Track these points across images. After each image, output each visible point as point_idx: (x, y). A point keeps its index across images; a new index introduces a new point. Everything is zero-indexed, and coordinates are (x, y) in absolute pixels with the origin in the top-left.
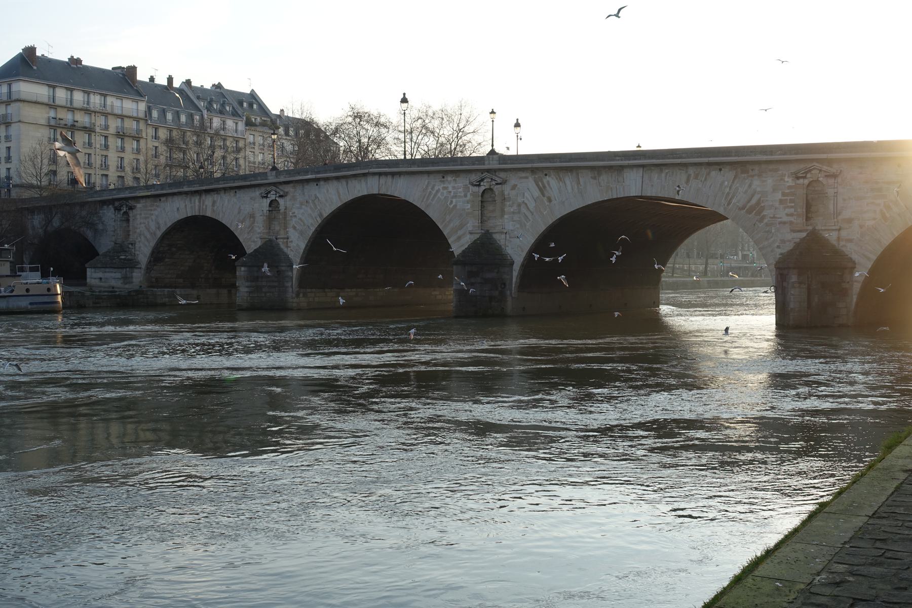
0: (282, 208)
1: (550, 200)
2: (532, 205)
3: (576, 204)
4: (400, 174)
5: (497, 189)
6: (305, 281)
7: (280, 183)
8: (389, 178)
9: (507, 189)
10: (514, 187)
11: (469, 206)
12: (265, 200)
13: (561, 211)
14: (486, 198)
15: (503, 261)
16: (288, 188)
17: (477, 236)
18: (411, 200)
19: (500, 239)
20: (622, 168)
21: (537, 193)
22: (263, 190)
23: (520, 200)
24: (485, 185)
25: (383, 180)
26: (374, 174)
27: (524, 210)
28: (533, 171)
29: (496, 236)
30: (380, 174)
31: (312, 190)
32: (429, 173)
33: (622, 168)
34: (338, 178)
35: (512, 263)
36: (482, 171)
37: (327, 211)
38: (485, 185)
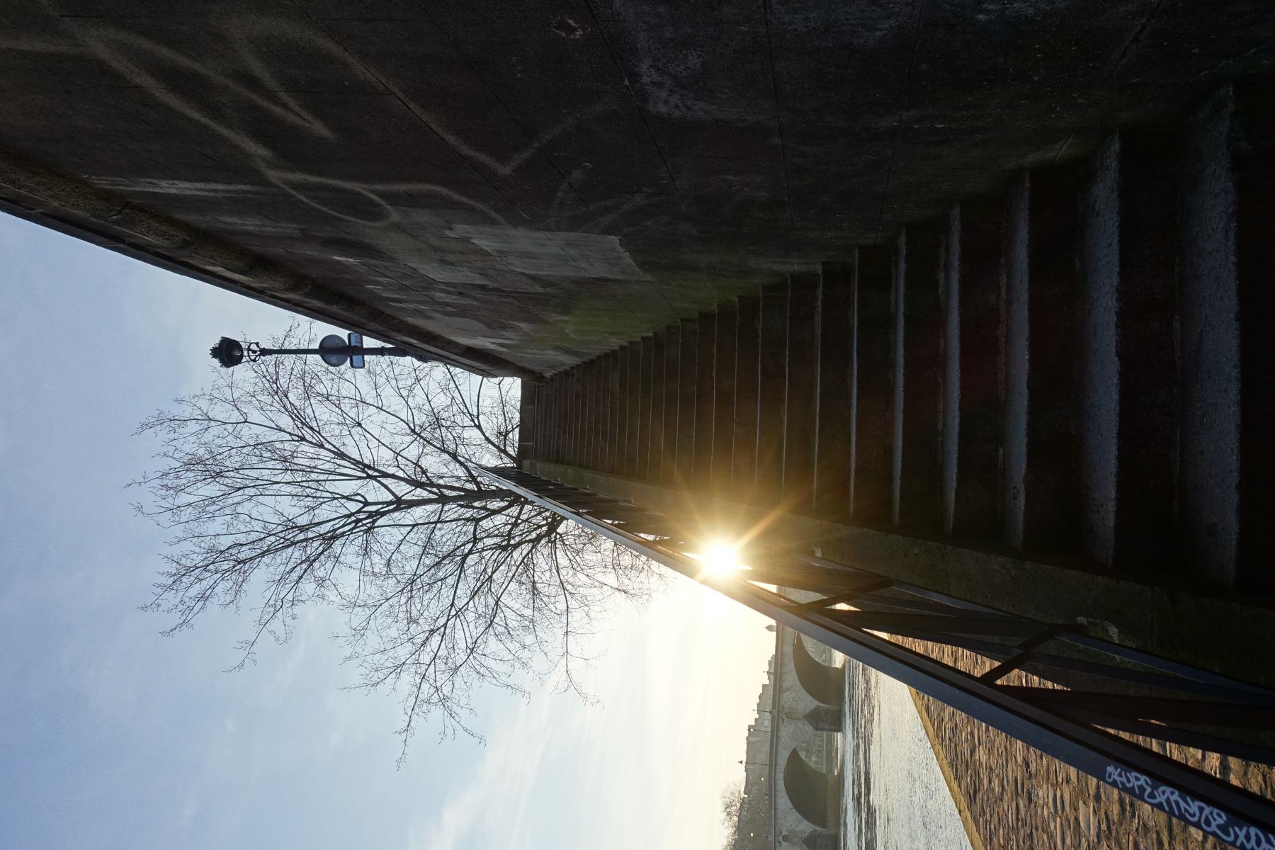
0: (787, 833)
1: (792, 686)
2: (794, 695)
3: (794, 674)
4: (776, 761)
5: (786, 711)
6: (824, 825)
7: (775, 832)
8: (778, 767)
9: (786, 706)
10: (786, 702)
11: (792, 726)
12: (782, 844)
13: (798, 682)
14: (790, 716)
15: (817, 709)
16: (778, 827)
17: (806, 722)
18: (788, 756)
19: (807, 711)
20: (782, 654)
21: (789, 692)
22: (778, 844)
23: (791, 700)
24: (784, 716)
25: (778, 770)
26: (775, 775)
27: (796, 699)
28: (780, 693)
29: (806, 712)
30: (775, 772)
31: (780, 812)
32: (777, 745)
33: (782, 654)
34: (775, 796)
35: (818, 706)
36: (778, 716)
37: (790, 805)
38: (784, 716)
